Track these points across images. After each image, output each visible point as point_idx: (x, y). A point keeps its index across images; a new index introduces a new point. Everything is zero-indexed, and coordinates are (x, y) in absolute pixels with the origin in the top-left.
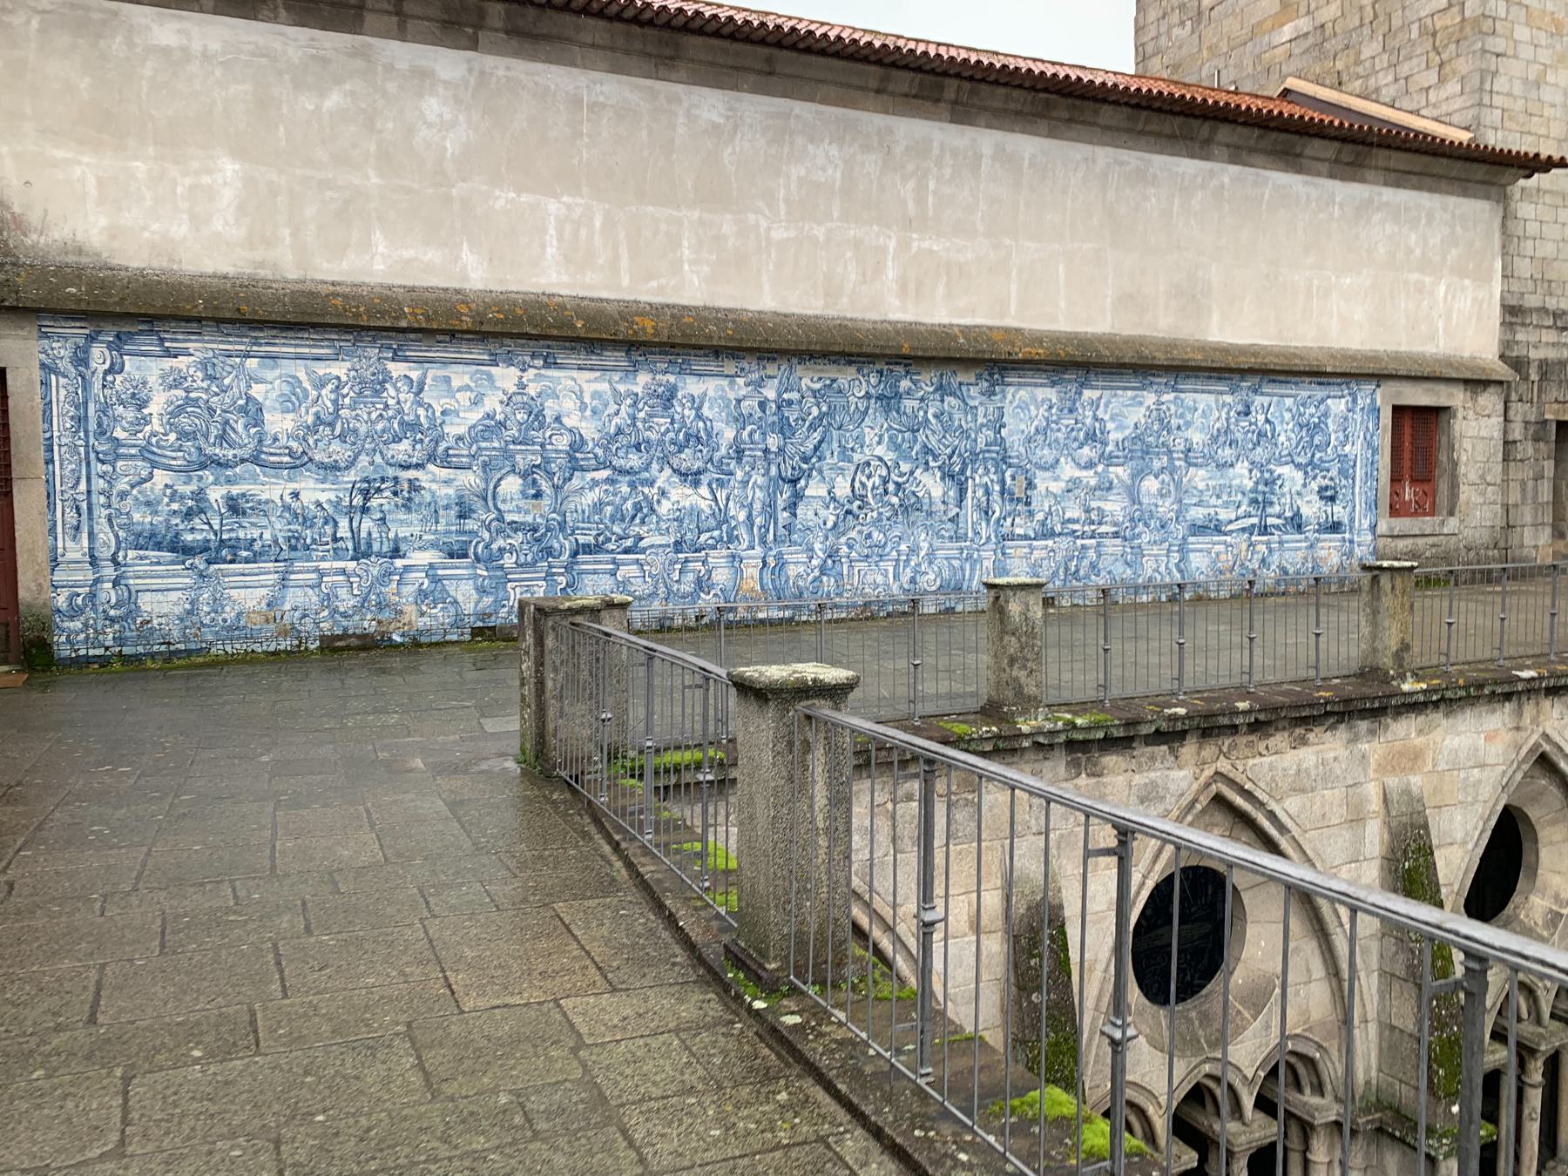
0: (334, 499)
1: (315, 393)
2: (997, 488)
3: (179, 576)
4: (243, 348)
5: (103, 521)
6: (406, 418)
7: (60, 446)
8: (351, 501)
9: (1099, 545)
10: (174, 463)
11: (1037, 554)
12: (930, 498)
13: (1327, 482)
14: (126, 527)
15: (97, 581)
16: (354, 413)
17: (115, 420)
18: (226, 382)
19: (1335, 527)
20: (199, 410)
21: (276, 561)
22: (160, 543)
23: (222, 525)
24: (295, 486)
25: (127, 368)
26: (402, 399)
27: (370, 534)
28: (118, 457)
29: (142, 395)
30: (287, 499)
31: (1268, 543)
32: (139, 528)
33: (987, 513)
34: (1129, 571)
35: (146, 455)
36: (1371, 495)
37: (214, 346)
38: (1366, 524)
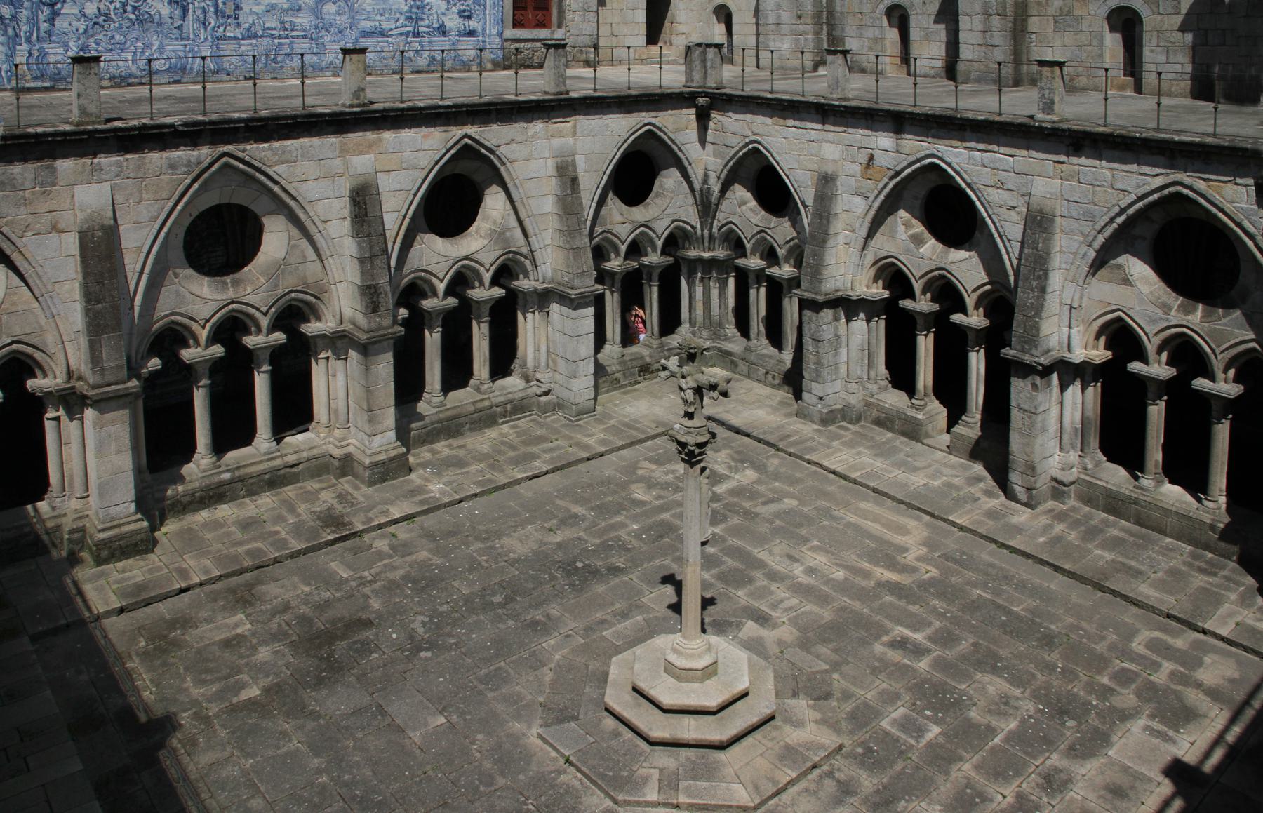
2: (212, 9)
9: (291, 43)
11: (243, 48)
12: (160, 15)
13: (462, 8)
19: (472, 33)
31: (420, 42)
33: (204, 24)
34: (315, 58)
36: (499, 16)
38: (495, 32)
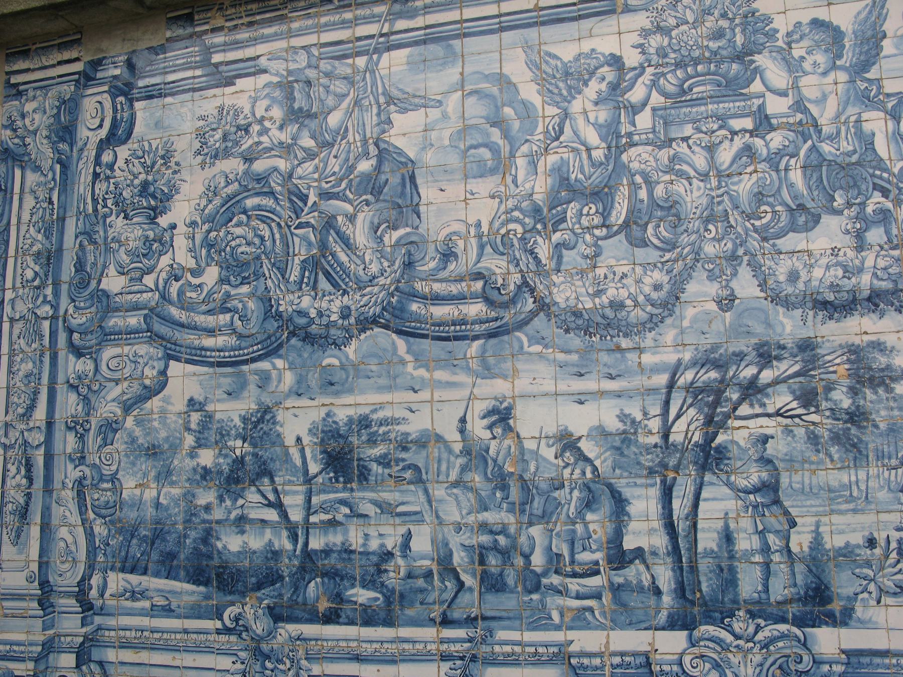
0: (613, 424)
1: (552, 111)
3: (209, 650)
4: (372, 29)
5: (69, 495)
6: (826, 148)
7: (12, 320)
8: (666, 436)
10: (209, 342)
14: (106, 512)
15: (49, 647)
16: (664, 155)
17: (108, 249)
18: (334, 120)
20: (268, 202)
21: (446, 622)
22: (172, 556)
23: (309, 509)
24: (500, 387)
25: (138, 129)
26: (811, 92)
27: (728, 537)
28: (108, 336)
29: (162, 185)
30: (478, 428)
32: (133, 515)
35: (159, 327)
37: (312, 39)
